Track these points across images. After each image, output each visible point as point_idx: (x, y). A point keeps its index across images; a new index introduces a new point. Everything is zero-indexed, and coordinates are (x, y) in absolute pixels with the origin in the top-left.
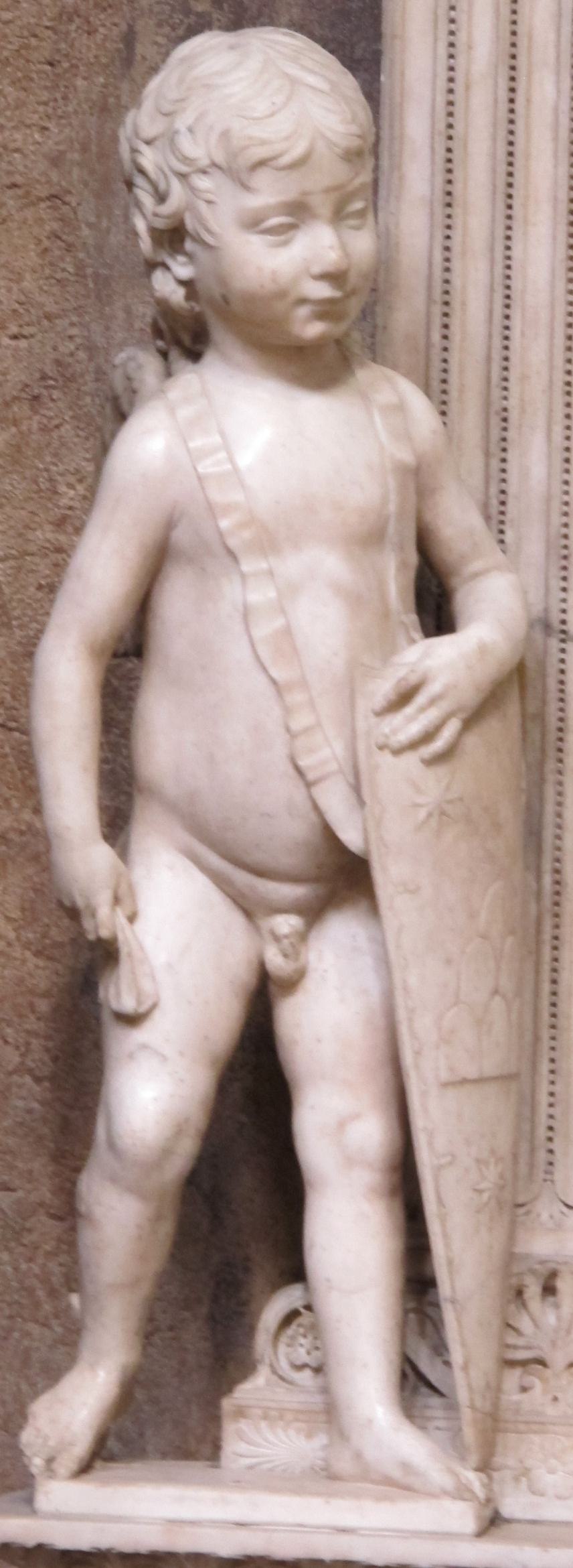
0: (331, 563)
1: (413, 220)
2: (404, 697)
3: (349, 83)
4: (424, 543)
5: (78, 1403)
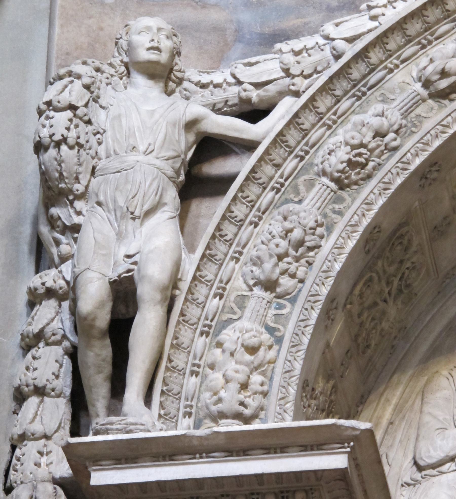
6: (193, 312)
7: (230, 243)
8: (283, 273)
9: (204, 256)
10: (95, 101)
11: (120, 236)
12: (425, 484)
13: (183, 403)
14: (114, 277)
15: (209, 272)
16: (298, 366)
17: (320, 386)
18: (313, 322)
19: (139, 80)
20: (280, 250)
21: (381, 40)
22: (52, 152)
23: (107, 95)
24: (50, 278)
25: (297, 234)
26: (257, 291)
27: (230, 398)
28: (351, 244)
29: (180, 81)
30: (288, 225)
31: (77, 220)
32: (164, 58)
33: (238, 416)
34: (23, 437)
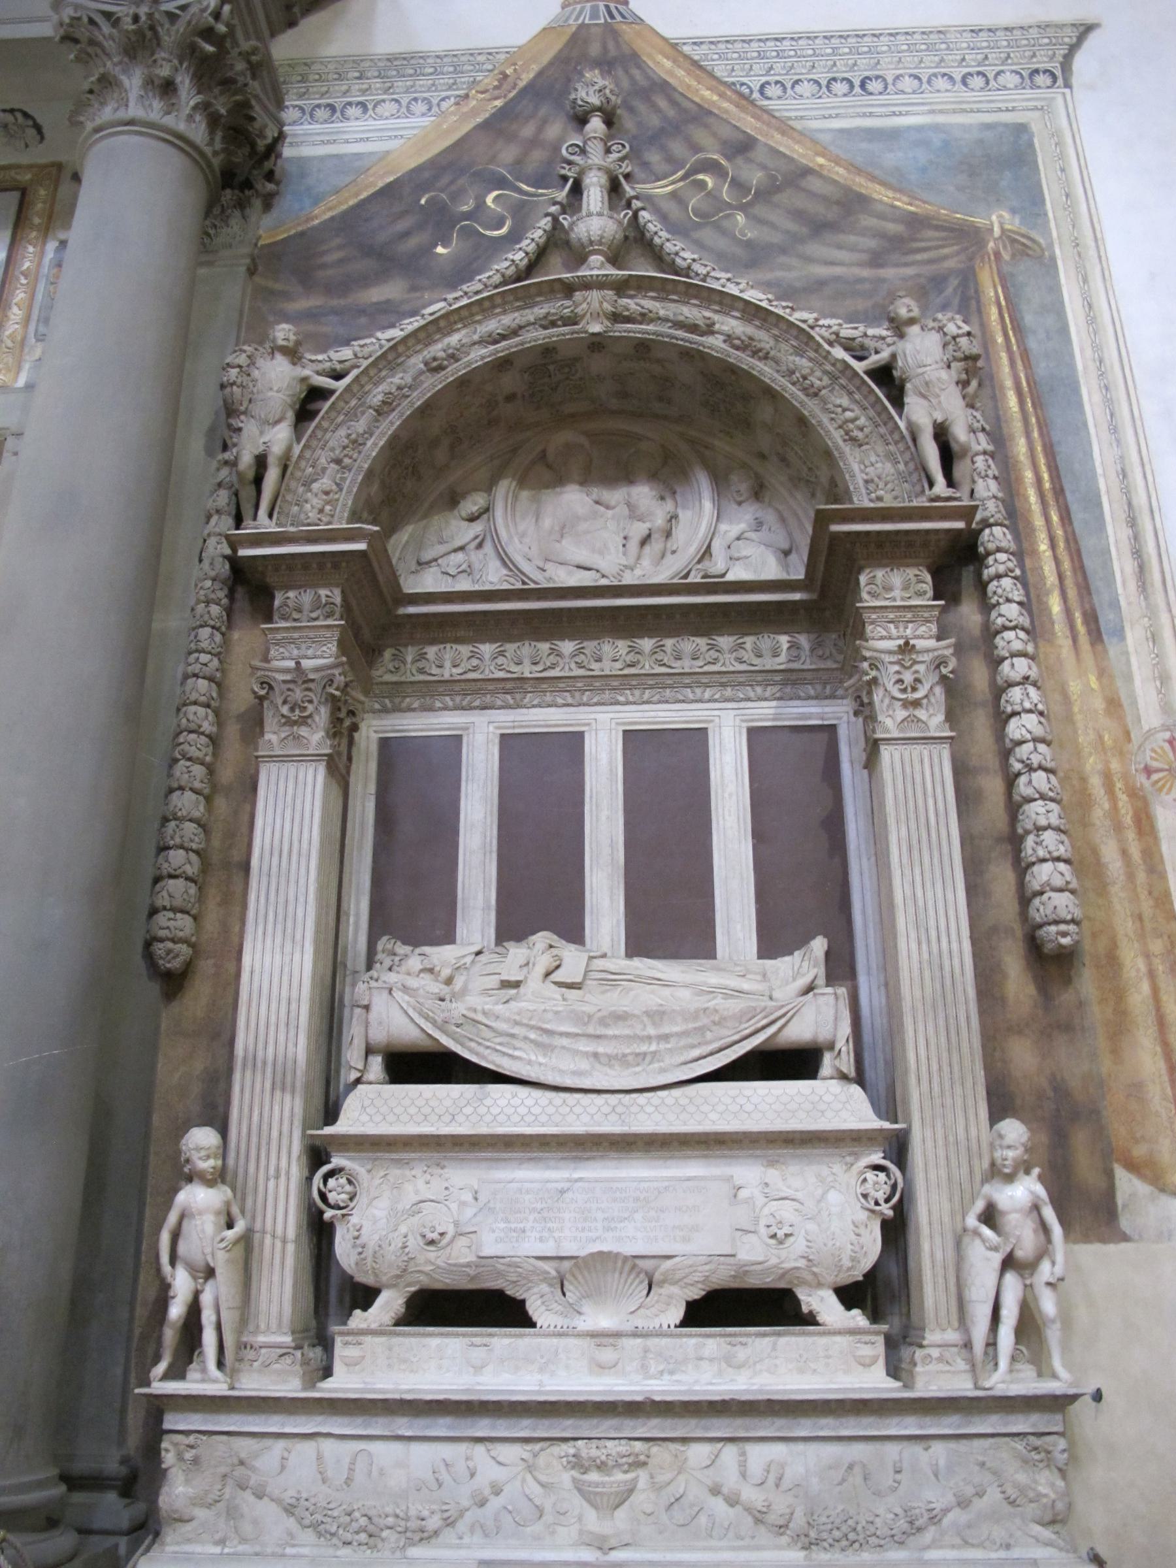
2: (222, 1240)
3: (219, 1136)
4: (229, 1214)
5: (162, 1367)
6: (298, 474)
7: (320, 440)
8: (346, 456)
10: (254, 364)
11: (262, 433)
14: (257, 453)
15: (308, 454)
16: (350, 503)
19: (279, 358)
21: (404, 340)
22: (228, 390)
23: (260, 362)
24: (227, 456)
25: (354, 436)
26: (333, 465)
27: (313, 515)
28: (382, 443)
29: (300, 358)
31: (241, 425)
32: (291, 344)
34: (209, 535)
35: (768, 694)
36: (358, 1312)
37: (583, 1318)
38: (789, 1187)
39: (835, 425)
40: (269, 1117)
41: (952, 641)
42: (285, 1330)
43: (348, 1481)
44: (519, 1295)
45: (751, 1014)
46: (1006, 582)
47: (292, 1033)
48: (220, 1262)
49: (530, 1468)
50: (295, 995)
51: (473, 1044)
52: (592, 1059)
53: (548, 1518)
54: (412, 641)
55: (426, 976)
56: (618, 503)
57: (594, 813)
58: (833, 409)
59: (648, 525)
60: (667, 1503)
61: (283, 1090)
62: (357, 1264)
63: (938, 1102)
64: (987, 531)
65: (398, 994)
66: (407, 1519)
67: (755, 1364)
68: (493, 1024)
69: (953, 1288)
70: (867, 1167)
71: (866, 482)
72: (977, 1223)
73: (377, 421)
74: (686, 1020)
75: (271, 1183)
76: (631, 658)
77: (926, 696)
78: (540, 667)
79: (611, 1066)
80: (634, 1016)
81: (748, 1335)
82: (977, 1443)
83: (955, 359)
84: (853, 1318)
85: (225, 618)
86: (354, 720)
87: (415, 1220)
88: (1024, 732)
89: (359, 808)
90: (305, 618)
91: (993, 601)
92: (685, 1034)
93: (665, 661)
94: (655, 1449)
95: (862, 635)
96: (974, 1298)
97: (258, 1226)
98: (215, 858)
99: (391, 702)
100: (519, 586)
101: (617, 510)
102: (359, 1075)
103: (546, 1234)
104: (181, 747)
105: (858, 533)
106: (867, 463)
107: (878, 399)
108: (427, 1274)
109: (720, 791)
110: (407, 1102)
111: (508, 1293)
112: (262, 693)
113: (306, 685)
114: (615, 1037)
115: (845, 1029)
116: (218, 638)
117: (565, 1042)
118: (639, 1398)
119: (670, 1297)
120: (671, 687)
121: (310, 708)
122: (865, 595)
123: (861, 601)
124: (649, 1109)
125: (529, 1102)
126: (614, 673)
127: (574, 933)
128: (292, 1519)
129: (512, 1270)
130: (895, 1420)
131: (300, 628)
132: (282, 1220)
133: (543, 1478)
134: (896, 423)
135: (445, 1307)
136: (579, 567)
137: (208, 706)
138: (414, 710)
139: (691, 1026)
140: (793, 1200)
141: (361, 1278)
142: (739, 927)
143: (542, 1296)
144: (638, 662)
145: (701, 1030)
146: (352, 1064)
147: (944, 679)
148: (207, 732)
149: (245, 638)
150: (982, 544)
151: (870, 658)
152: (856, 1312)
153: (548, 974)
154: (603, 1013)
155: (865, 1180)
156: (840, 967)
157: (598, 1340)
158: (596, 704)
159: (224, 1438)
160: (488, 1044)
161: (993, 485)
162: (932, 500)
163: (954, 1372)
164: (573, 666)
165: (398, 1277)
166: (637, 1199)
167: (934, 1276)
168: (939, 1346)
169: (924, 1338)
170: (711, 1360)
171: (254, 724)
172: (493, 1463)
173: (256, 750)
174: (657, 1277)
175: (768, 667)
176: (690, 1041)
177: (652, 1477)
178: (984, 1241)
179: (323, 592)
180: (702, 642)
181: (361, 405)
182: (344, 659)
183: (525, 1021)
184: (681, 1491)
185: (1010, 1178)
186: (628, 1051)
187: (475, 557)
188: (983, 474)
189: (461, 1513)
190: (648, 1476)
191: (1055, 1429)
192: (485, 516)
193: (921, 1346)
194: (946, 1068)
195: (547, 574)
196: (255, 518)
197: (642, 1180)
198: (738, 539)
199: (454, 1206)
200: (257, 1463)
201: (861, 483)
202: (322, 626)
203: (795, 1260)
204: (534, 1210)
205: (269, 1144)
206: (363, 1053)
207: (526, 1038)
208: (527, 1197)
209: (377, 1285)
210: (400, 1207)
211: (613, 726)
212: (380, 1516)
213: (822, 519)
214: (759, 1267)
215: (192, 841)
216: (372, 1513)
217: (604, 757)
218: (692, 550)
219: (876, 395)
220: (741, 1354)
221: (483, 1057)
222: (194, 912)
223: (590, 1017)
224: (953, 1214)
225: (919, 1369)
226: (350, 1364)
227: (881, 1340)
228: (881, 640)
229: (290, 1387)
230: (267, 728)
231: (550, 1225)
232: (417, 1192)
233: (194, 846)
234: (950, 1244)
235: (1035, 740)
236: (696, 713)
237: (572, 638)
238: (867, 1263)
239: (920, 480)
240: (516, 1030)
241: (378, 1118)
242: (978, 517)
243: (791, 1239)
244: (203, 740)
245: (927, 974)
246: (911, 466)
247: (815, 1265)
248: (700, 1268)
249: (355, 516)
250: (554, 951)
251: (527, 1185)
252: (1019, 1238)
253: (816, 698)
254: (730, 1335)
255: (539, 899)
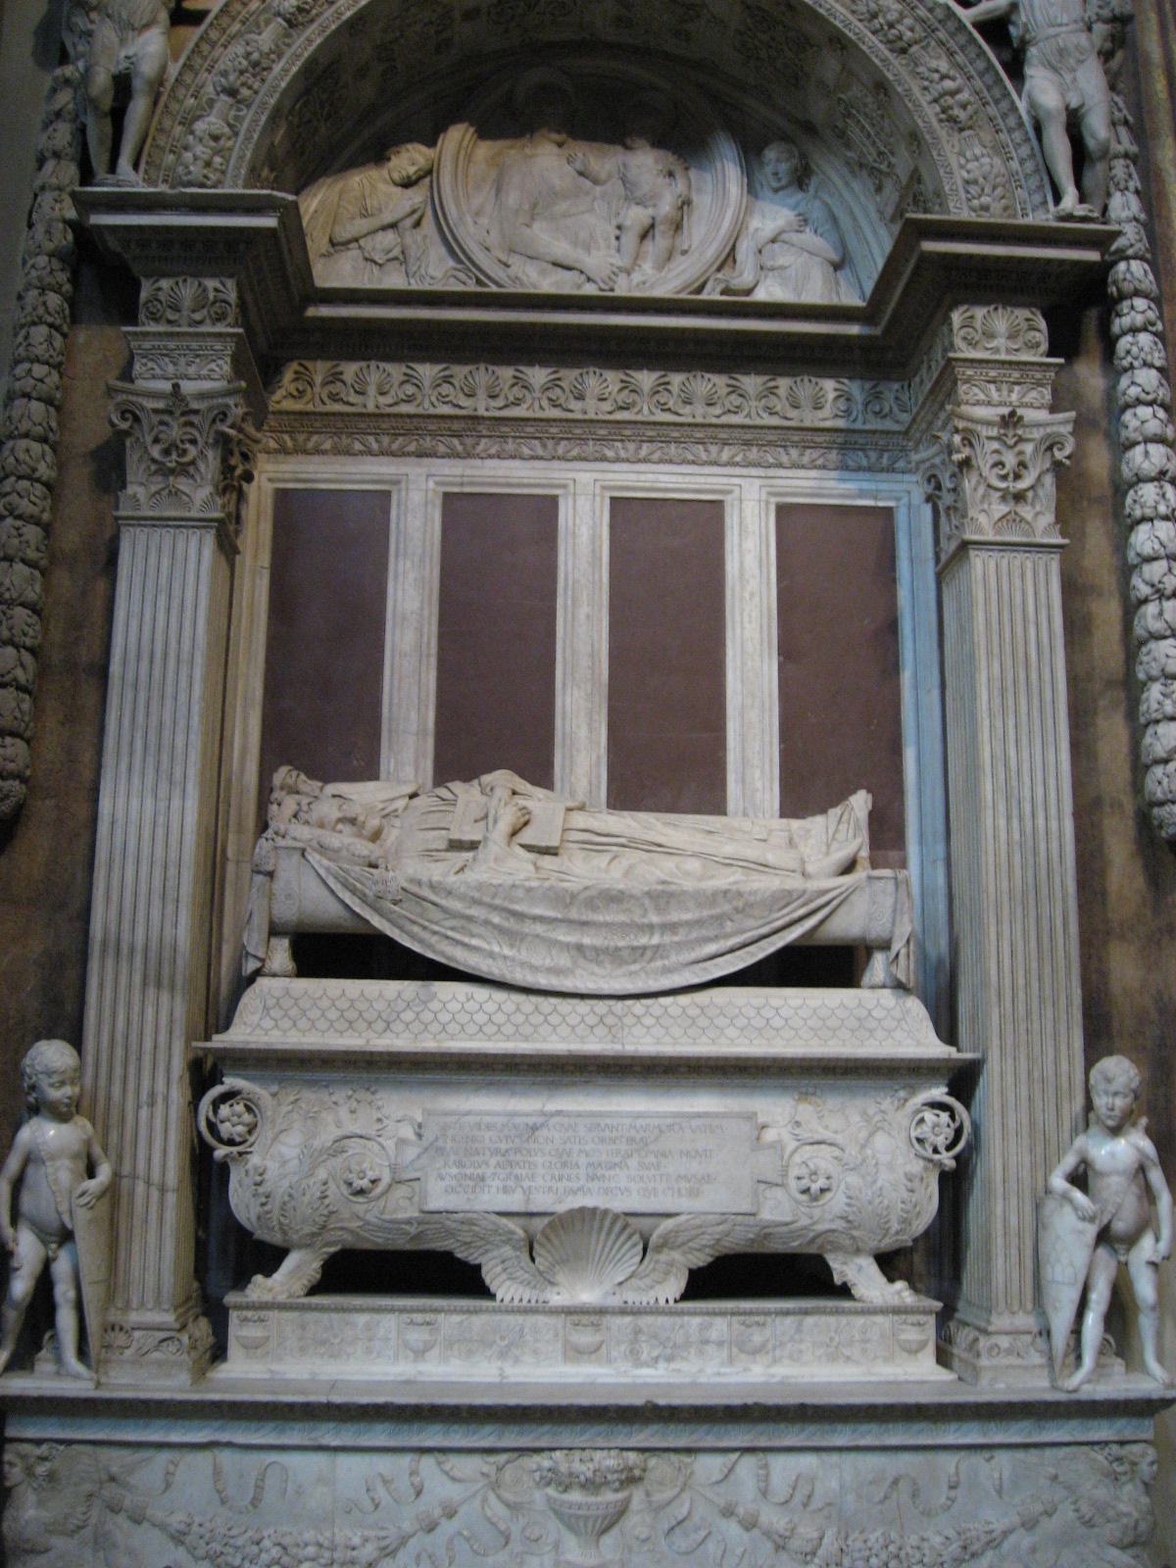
0: (67, 1163)
1: (88, 1080)
2: (83, 1194)
3: (75, 1053)
6: (174, 107)
7: (205, 58)
8: (243, 84)
9: (185, 65)
11: (122, 42)
12: (336, 256)
13: (162, 173)
14: (114, 70)
15: (188, 78)
16: (249, 154)
17: (265, 172)
18: (262, 123)
20: (242, 67)
24: (68, 71)
25: (255, 56)
26: (223, 97)
27: (197, 170)
28: (295, 69)
30: (249, 49)
31: (90, 27)
33: (202, 186)
34: (43, 188)
35: (806, 460)
36: (259, 1278)
37: (556, 1289)
38: (826, 1127)
39: (929, 98)
40: (139, 1023)
41: (1073, 414)
42: (166, 1307)
43: (255, 1502)
44: (473, 1258)
45: (786, 898)
46: (1144, 338)
47: (170, 907)
48: (82, 1223)
49: (495, 1486)
50: (173, 855)
51: (416, 929)
52: (574, 952)
53: (516, 1546)
54: (322, 352)
55: (347, 829)
56: (610, 176)
57: (570, 609)
58: (927, 74)
59: (650, 211)
60: (666, 1527)
61: (159, 985)
62: (259, 1218)
63: (1023, 1027)
64: (1122, 266)
65: (314, 857)
66: (333, 1549)
67: (774, 1349)
68: (443, 902)
69: (1029, 1263)
70: (925, 1105)
71: (967, 182)
72: (1066, 1185)
73: (288, 36)
74: (700, 905)
75: (144, 1113)
76: (625, 397)
77: (1032, 487)
78: (500, 402)
79: (599, 963)
80: (632, 896)
81: (767, 1313)
82: (1048, 1452)
83: (1099, 19)
84: (899, 1293)
85: (67, 312)
86: (248, 467)
87: (337, 1162)
88: (1157, 546)
89: (246, 587)
90: (184, 321)
91: (1125, 363)
92: (699, 923)
93: (671, 404)
94: (653, 1462)
95: (951, 394)
96: (1059, 1277)
97: (126, 1169)
98: (56, 657)
99: (292, 439)
100: (472, 287)
101: (608, 186)
102: (258, 964)
103: (511, 1183)
104: (8, 499)
105: (957, 256)
106: (968, 154)
107: (990, 66)
108: (351, 1232)
109: (737, 588)
110: (325, 1003)
111: (459, 1255)
112: (125, 426)
113: (183, 419)
114: (607, 925)
115: (904, 929)
116: (58, 341)
117: (539, 929)
118: (639, 1401)
119: (671, 1264)
120: (677, 441)
121: (192, 451)
122: (958, 342)
123: (952, 347)
124: (648, 1021)
125: (490, 1007)
126: (601, 417)
127: (540, 772)
128: (181, 1549)
129: (465, 1228)
130: (954, 1426)
131: (178, 334)
132: (162, 1160)
133: (508, 1496)
134: (1013, 103)
135: (369, 1270)
136: (555, 264)
137: (44, 440)
138: (324, 452)
139: (706, 913)
140: (831, 1144)
141: (260, 1234)
142: (757, 774)
143: (503, 1262)
144: (634, 404)
145: (719, 919)
146: (250, 950)
147: (1057, 465)
148: (44, 479)
149: (97, 343)
150: (1115, 282)
151: (965, 430)
152: (900, 1285)
153: (514, 833)
154: (593, 892)
155: (922, 1121)
156: (886, 834)
157: (575, 1318)
158: (575, 459)
159: (88, 1449)
160: (436, 928)
161: (1135, 205)
162: (1062, 219)
163: (1026, 1368)
164: (545, 403)
165: (313, 1235)
166: (631, 1140)
167: (1007, 1246)
168: (1007, 1333)
169: (988, 1322)
170: (720, 1344)
171: (109, 467)
172: (444, 1478)
173: (117, 508)
174: (654, 1239)
175: (807, 424)
176: (704, 932)
177: (648, 1494)
178: (1076, 1209)
179: (211, 284)
180: (720, 381)
181: (265, 10)
182: (243, 384)
183: (487, 899)
184: (684, 1511)
185: (1116, 1131)
186: (621, 944)
187: (413, 239)
188: (1122, 186)
189: (404, 1540)
190: (643, 1496)
191: (1144, 1436)
192: (427, 180)
193: (985, 1332)
194: (1035, 985)
195: (512, 271)
196: (112, 168)
197: (639, 1115)
198: (773, 241)
199: (390, 1144)
200: (132, 1480)
201: (960, 183)
202: (210, 335)
203: (832, 1220)
204: (497, 1151)
205: (139, 1059)
206: (265, 935)
207: (487, 923)
208: (487, 1135)
209: (285, 1245)
210: (317, 1143)
211: (598, 491)
212: (298, 1545)
213: (914, 232)
214: (785, 1229)
215: (25, 635)
216: (287, 1541)
217: (584, 532)
218: (712, 251)
219: (988, 60)
220: (757, 1338)
221: (430, 946)
222: (28, 734)
223: (573, 896)
224: (1033, 1166)
225: (984, 1362)
226: (252, 1347)
227: (931, 1320)
228: (981, 404)
229: (173, 1384)
230: (130, 478)
231: (517, 1171)
232: (339, 1124)
233: (28, 642)
234: (1028, 1208)
235: (1168, 557)
236: (710, 480)
237: (543, 363)
238: (920, 1225)
239: (1041, 187)
240: (473, 912)
241: (286, 1024)
242: (1113, 248)
243: (828, 1195)
244: (39, 489)
245: (1017, 859)
246: (1029, 166)
247: (855, 1228)
248: (710, 1230)
249: (254, 176)
250: (521, 801)
251: (487, 1119)
252: (1119, 1207)
253: (869, 469)
254: (745, 1313)
255: (493, 726)
